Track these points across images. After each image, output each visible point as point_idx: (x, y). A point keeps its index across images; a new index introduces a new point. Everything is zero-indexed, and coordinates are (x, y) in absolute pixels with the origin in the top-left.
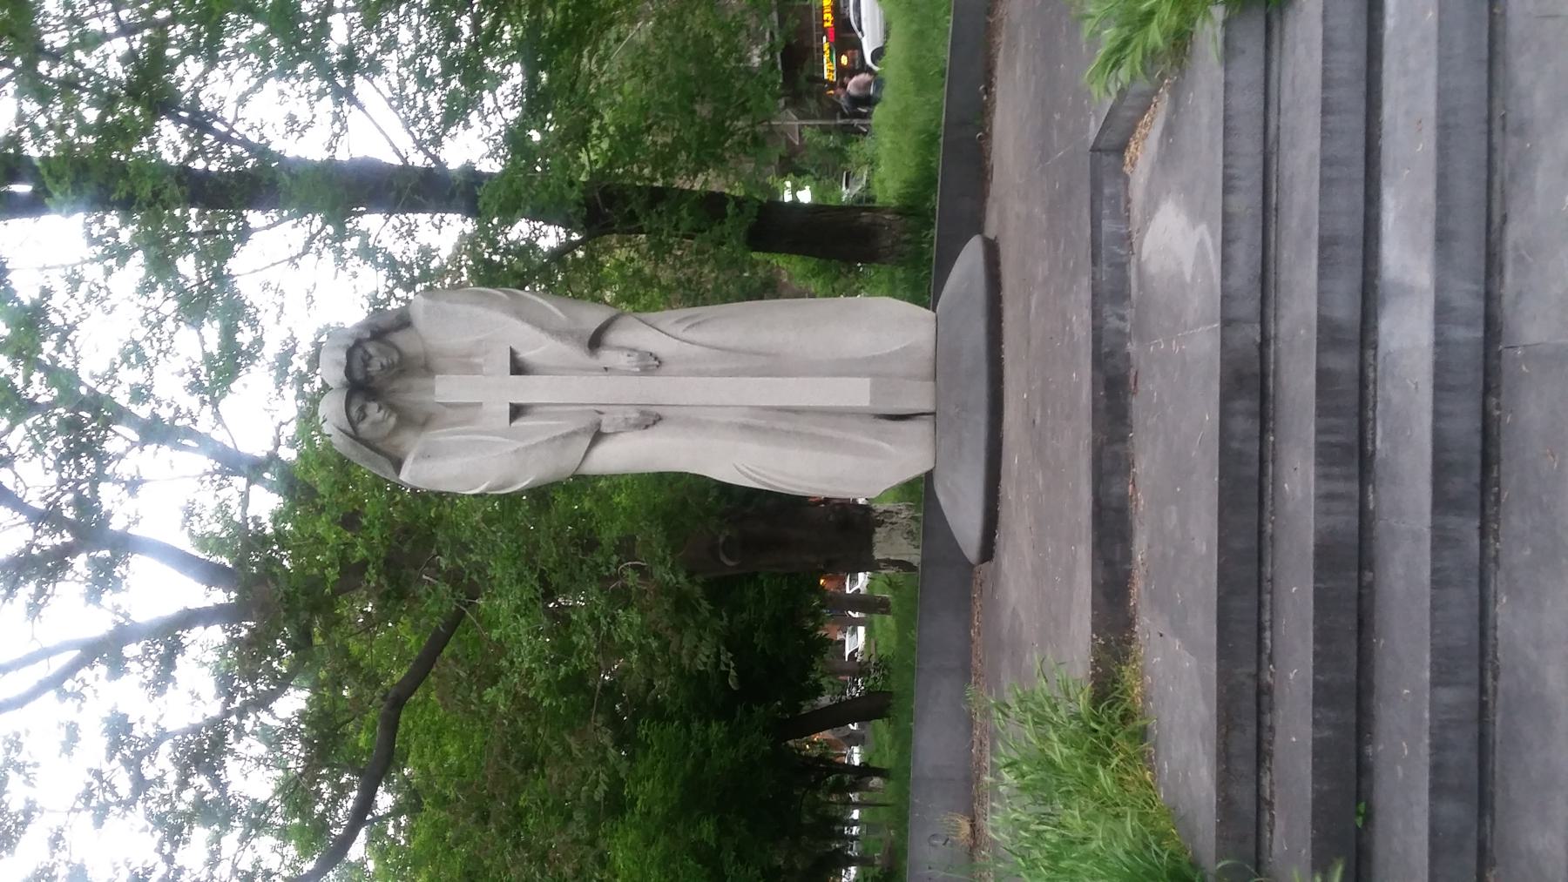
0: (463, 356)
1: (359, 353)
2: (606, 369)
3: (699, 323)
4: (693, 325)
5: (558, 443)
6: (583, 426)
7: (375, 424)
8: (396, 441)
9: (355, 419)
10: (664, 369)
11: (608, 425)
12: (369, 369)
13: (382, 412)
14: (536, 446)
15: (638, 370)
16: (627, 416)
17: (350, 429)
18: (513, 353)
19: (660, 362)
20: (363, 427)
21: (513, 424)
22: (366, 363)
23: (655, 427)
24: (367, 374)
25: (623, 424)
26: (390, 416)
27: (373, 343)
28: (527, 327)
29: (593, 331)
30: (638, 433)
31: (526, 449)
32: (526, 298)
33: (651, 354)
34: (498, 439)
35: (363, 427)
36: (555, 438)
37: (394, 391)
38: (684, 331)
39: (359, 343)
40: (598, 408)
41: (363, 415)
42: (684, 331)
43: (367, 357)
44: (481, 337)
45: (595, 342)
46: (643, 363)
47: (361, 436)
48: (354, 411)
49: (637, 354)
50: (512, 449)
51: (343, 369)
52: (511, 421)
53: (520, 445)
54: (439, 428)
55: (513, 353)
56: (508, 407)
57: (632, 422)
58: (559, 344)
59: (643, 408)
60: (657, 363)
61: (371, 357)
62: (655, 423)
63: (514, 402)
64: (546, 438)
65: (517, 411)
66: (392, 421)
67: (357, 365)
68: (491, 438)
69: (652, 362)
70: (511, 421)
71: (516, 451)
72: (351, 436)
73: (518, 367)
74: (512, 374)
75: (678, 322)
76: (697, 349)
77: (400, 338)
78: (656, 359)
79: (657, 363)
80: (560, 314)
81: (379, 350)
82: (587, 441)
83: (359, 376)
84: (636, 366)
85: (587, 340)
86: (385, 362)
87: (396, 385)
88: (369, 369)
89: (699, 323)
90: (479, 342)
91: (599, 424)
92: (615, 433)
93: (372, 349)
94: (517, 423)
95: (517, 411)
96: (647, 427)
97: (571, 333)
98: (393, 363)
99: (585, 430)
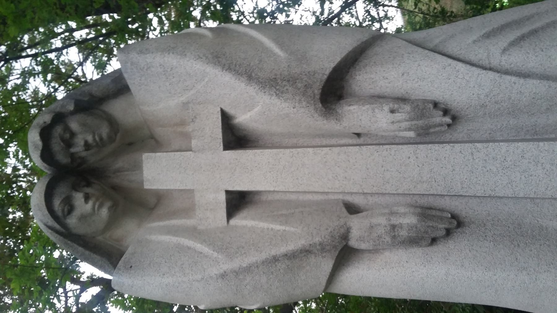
0: (177, 125)
1: (58, 130)
2: (358, 135)
3: (534, 32)
4: (522, 38)
5: (281, 266)
6: (317, 240)
7: (83, 218)
8: (118, 232)
9: (60, 214)
10: (461, 130)
11: (361, 239)
12: (73, 150)
13: (90, 203)
14: (248, 269)
15: (412, 134)
16: (395, 221)
18: (226, 118)
19: (454, 118)
20: (72, 221)
21: (233, 222)
22: (68, 144)
23: (451, 244)
24: (72, 156)
25: (388, 239)
26: (101, 206)
27: (78, 117)
28: (227, 78)
29: (328, 72)
30: (417, 251)
31: (237, 273)
32: (233, 31)
33: (436, 105)
34: (206, 250)
35: (72, 221)
36: (275, 259)
37: (119, 171)
38: (504, 51)
40: (349, 198)
41: (71, 209)
42: (504, 51)
43: (67, 136)
44: (183, 99)
46: (420, 123)
47: (74, 231)
48: (57, 203)
49: (408, 108)
50: (215, 271)
51: (39, 152)
52: (228, 221)
53: (226, 266)
54: (161, 218)
55: (226, 118)
56: (223, 197)
57: (404, 233)
58: (275, 101)
59: (423, 201)
60: (448, 120)
61: (73, 135)
62: (448, 233)
63: (230, 189)
64: (264, 256)
66: (104, 212)
68: (199, 246)
69: (438, 118)
71: (223, 276)
74: (227, 147)
75: (488, 36)
76: (533, 85)
78: (446, 112)
79: (448, 120)
80: (277, 50)
81: (83, 125)
82: (327, 265)
84: (410, 129)
85: (318, 92)
86: (90, 138)
87: (120, 163)
88: (73, 150)
89: (534, 32)
90: (185, 105)
91: (345, 237)
92: (375, 251)
93: (74, 125)
96: (434, 241)
97: (292, 80)
98: (101, 139)
99: (323, 248)
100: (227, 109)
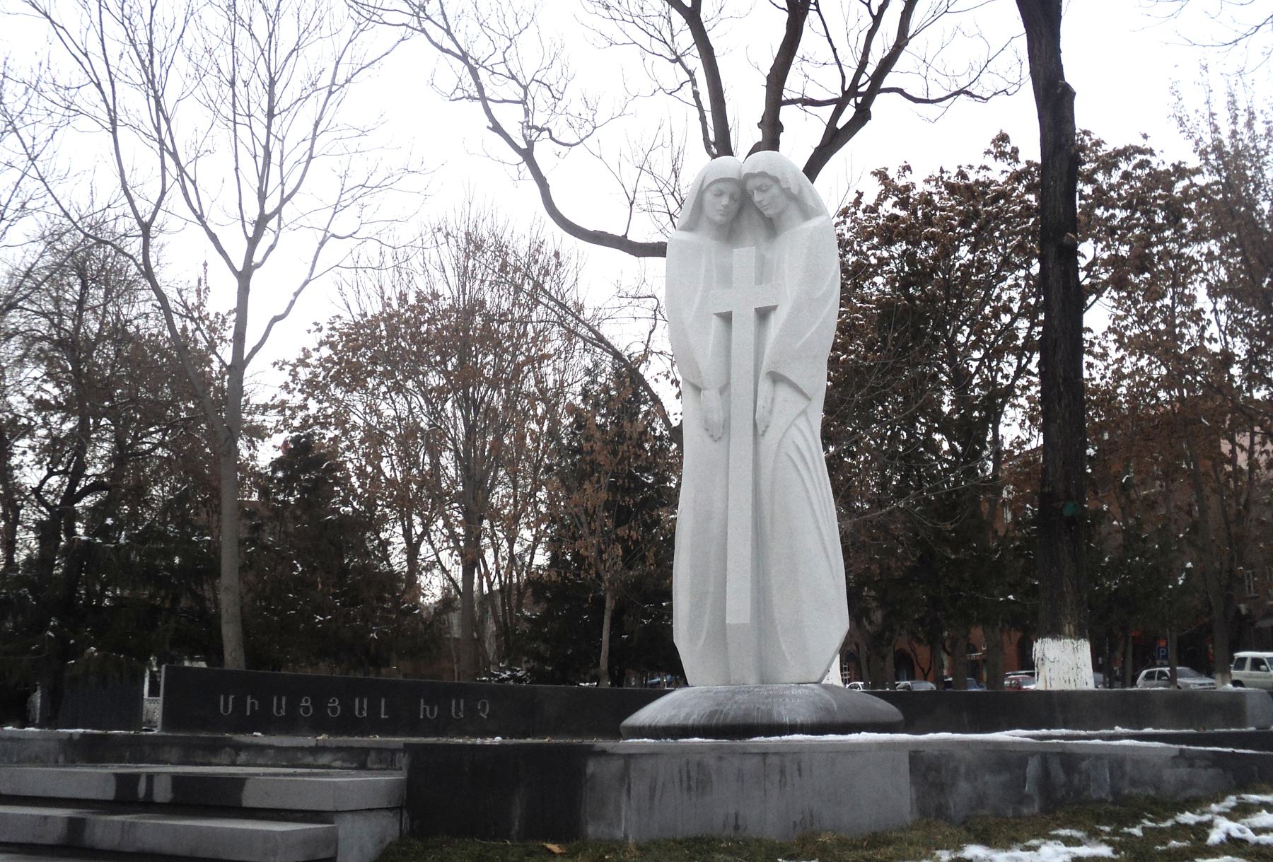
1: (768, 182)
17: (705, 186)
18: (774, 308)
22: (759, 189)
33: (767, 427)
39: (776, 180)
45: (776, 378)
48: (721, 186)
52: (717, 314)
55: (774, 308)
65: (727, 318)
67: (758, 182)
70: (717, 314)
72: (702, 185)
73: (763, 315)
77: (793, 211)
83: (751, 184)
94: (715, 323)
95: (727, 318)
96: (707, 430)
100: (778, 309)
